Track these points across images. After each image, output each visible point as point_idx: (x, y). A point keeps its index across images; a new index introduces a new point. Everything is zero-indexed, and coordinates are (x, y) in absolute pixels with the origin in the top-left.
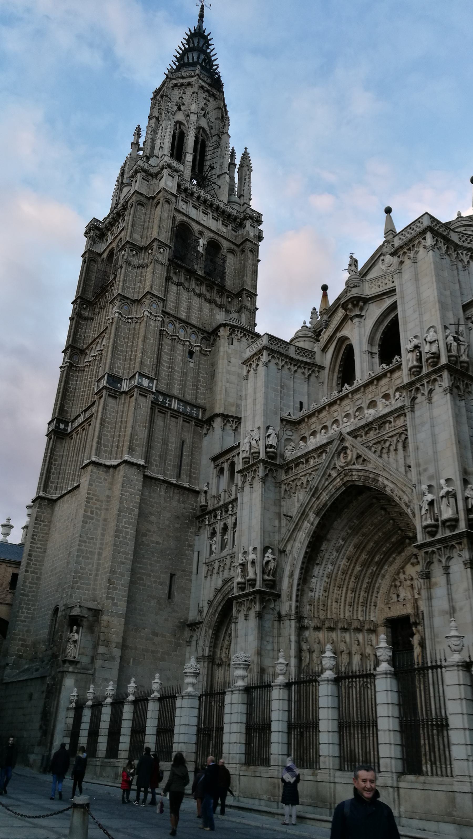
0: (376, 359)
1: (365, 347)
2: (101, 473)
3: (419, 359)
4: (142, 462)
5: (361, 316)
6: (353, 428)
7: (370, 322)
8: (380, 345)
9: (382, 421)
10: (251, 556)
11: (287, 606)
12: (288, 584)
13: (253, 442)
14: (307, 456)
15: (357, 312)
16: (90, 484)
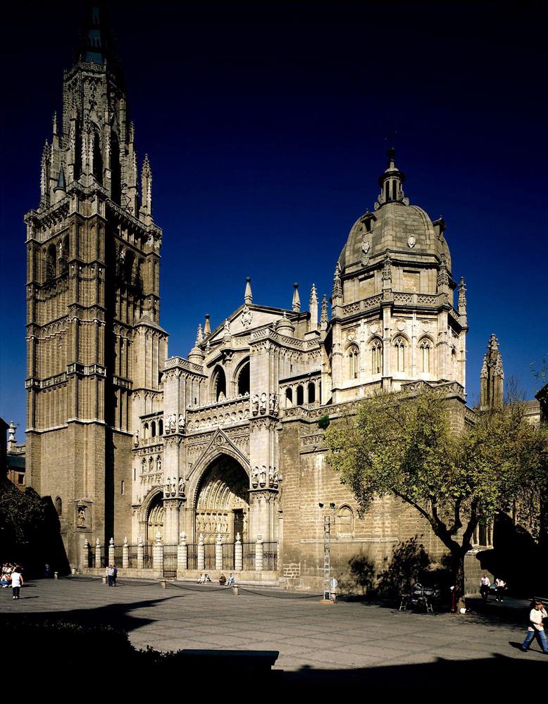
0: (237, 387)
1: (232, 379)
2: (80, 426)
3: (257, 408)
4: (103, 422)
5: (230, 360)
6: (224, 427)
7: (235, 365)
8: (239, 379)
9: (238, 427)
10: (173, 482)
11: (189, 504)
12: (190, 495)
13: (172, 423)
14: (201, 435)
15: (228, 357)
16: (76, 435)
